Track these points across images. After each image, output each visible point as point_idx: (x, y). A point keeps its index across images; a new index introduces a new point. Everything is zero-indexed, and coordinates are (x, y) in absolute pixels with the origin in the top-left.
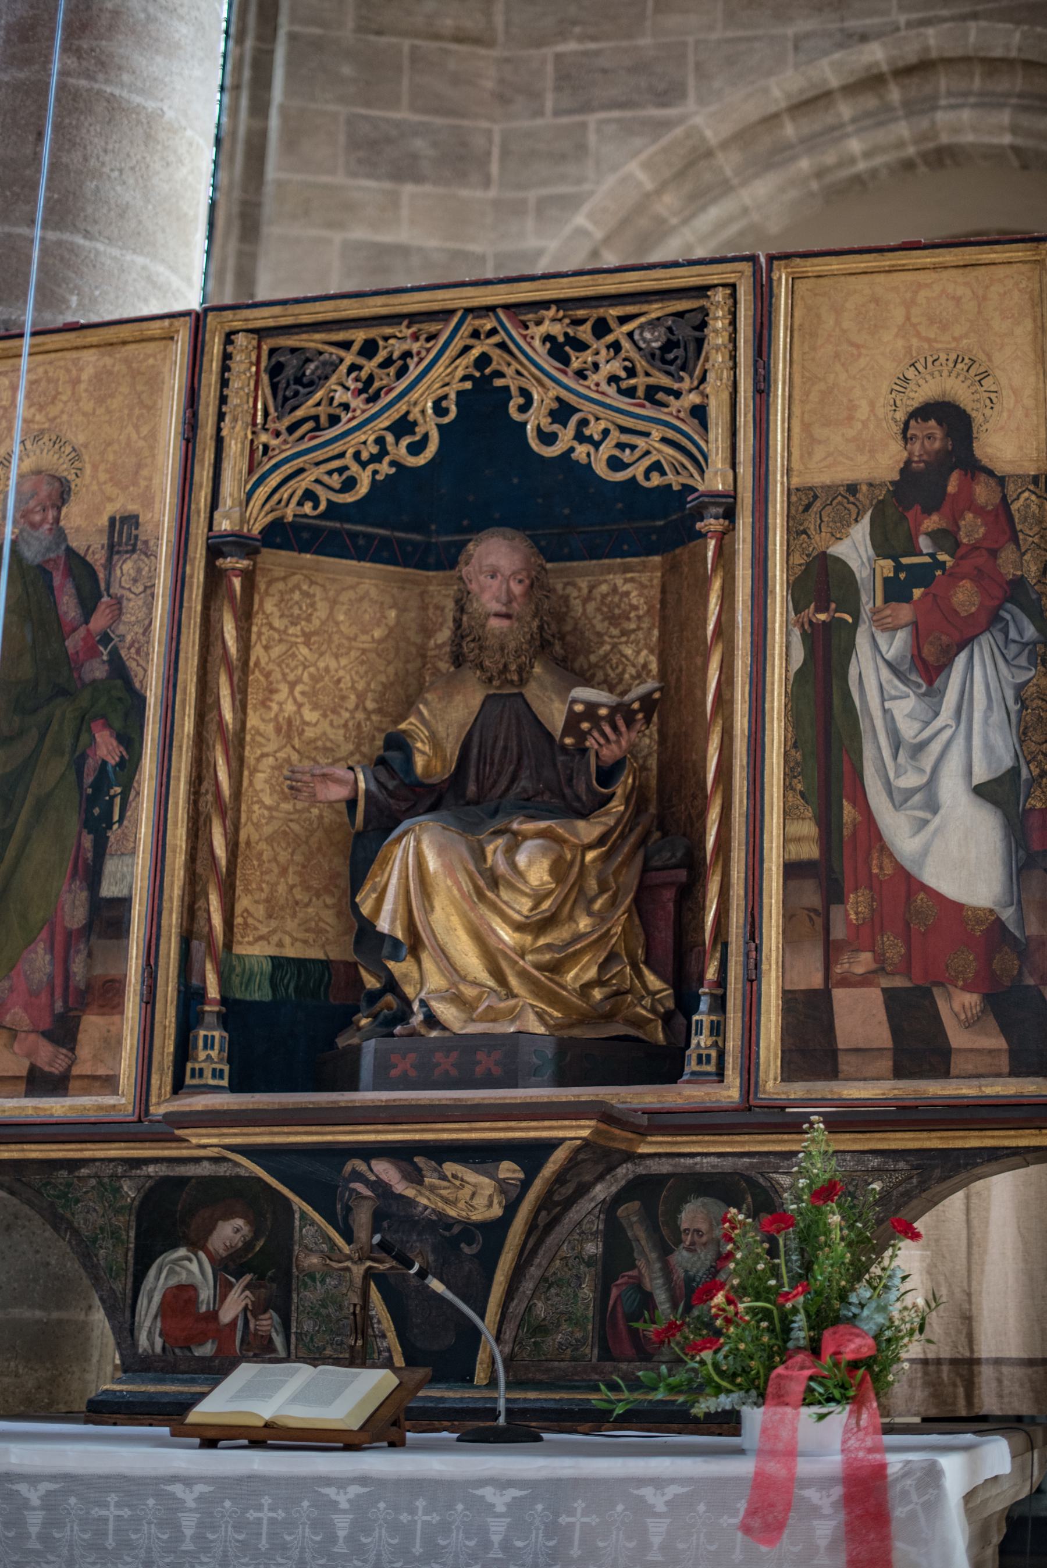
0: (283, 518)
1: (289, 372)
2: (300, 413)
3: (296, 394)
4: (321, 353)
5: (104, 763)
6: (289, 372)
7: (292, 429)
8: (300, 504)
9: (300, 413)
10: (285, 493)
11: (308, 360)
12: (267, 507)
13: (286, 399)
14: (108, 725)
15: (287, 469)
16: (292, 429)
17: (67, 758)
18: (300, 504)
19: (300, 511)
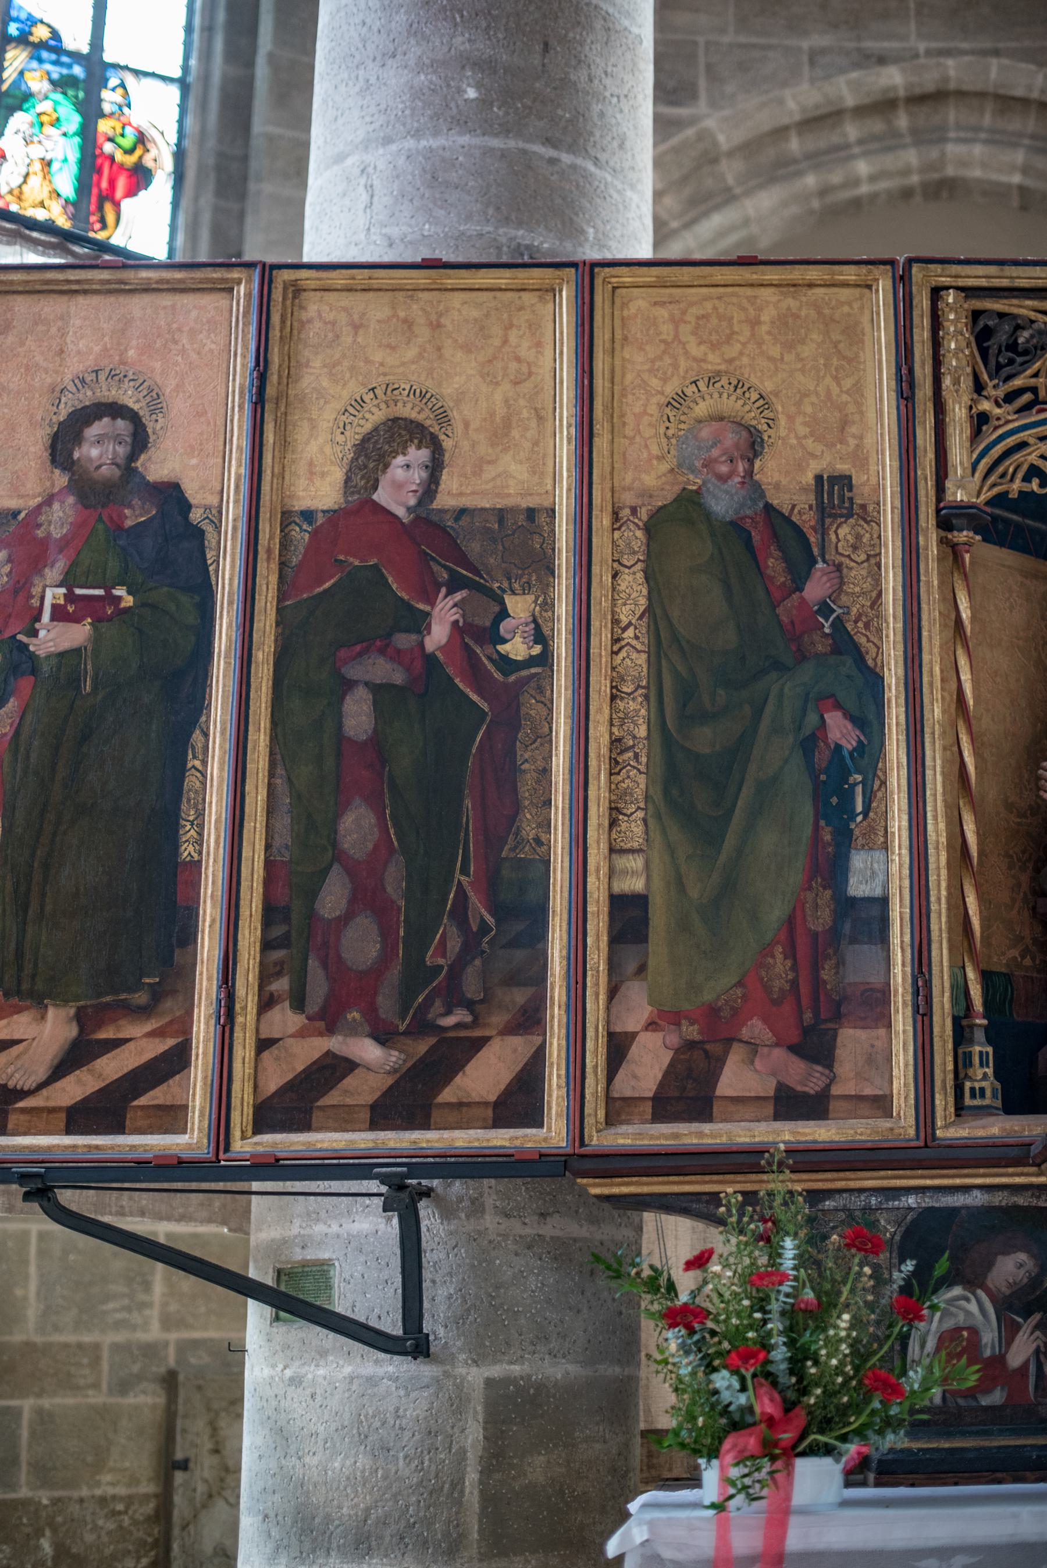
0: (1007, 493)
1: (1002, 337)
2: (1018, 382)
3: (1011, 362)
4: (1032, 322)
5: (838, 747)
6: (1002, 337)
7: (1010, 397)
8: (1027, 479)
9: (1018, 382)
10: (1009, 465)
11: (1018, 328)
12: (993, 479)
13: (999, 367)
14: (838, 706)
15: (1010, 441)
16: (1010, 397)
17: (791, 739)
18: (1027, 479)
19: (1026, 487)
